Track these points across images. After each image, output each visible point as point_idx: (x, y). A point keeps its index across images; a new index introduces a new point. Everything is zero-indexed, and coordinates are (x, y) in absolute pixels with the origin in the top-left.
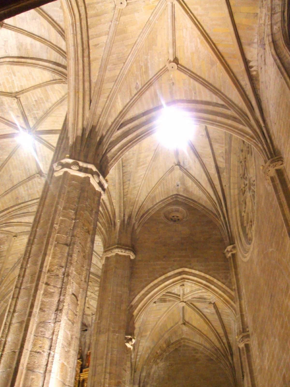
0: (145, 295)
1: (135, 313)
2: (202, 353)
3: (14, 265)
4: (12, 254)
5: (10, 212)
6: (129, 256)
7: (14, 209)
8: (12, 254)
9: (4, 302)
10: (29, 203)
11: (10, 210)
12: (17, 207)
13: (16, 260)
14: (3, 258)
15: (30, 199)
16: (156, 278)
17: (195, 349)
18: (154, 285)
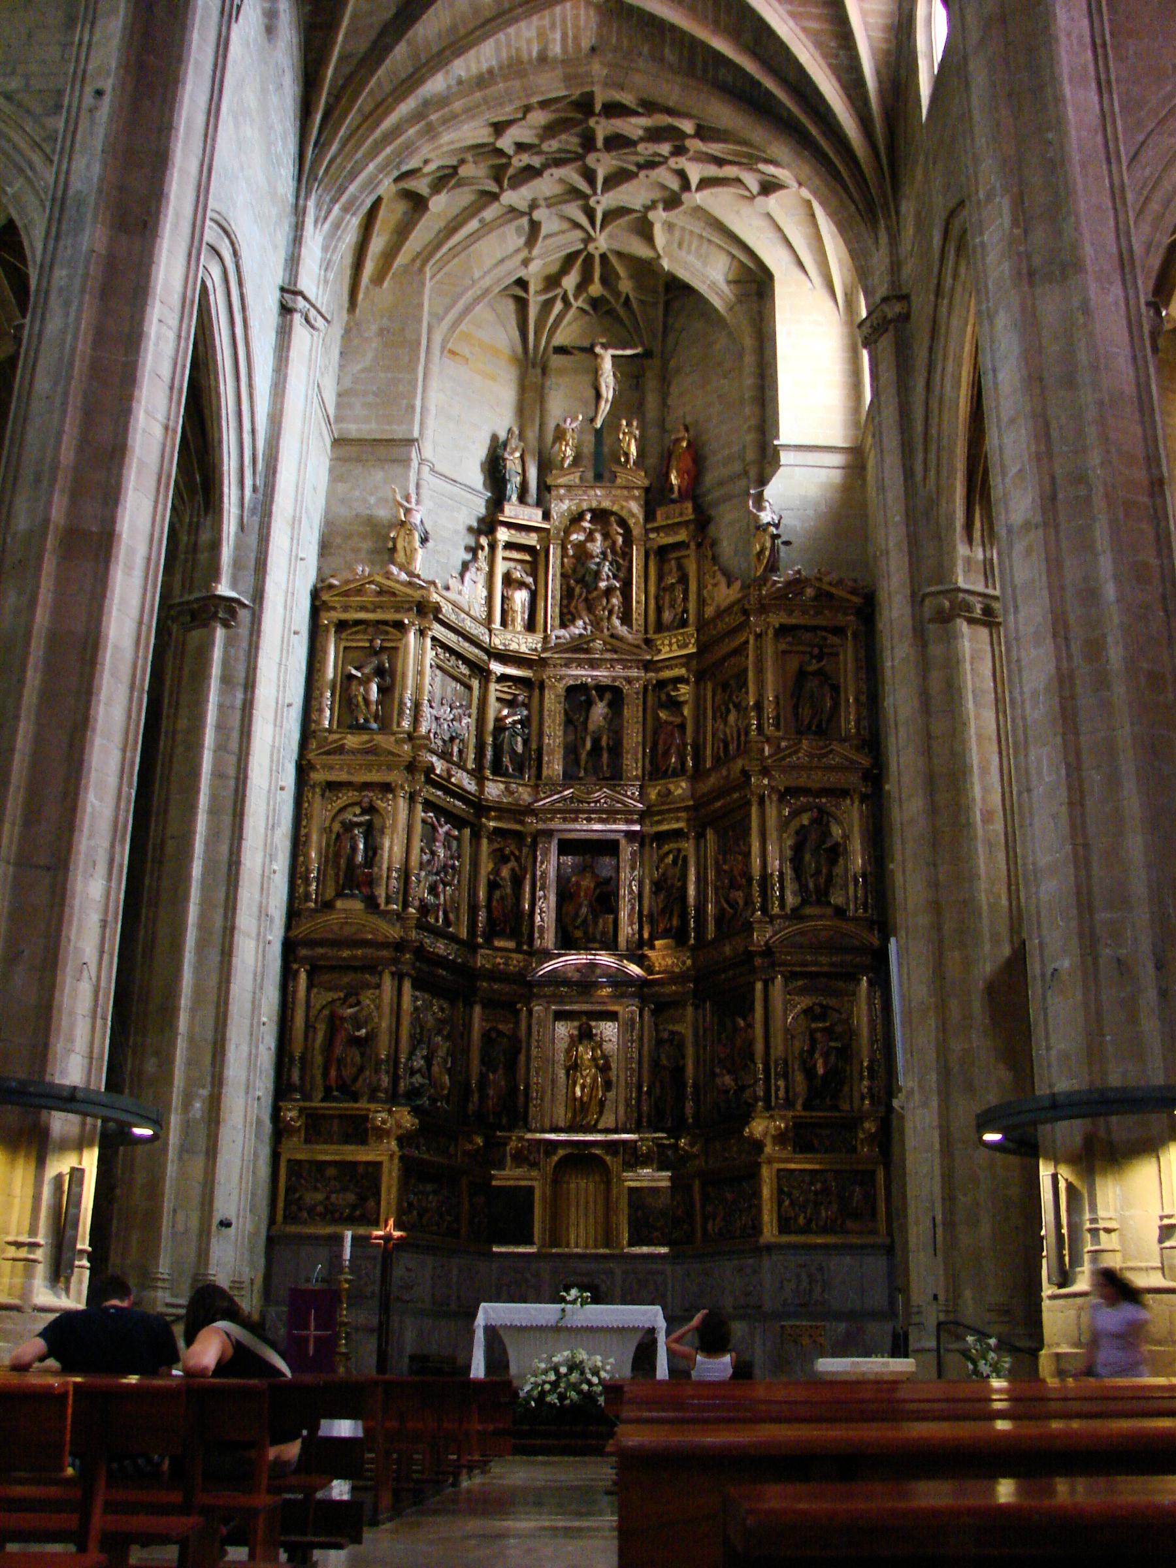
3: (372, 35)
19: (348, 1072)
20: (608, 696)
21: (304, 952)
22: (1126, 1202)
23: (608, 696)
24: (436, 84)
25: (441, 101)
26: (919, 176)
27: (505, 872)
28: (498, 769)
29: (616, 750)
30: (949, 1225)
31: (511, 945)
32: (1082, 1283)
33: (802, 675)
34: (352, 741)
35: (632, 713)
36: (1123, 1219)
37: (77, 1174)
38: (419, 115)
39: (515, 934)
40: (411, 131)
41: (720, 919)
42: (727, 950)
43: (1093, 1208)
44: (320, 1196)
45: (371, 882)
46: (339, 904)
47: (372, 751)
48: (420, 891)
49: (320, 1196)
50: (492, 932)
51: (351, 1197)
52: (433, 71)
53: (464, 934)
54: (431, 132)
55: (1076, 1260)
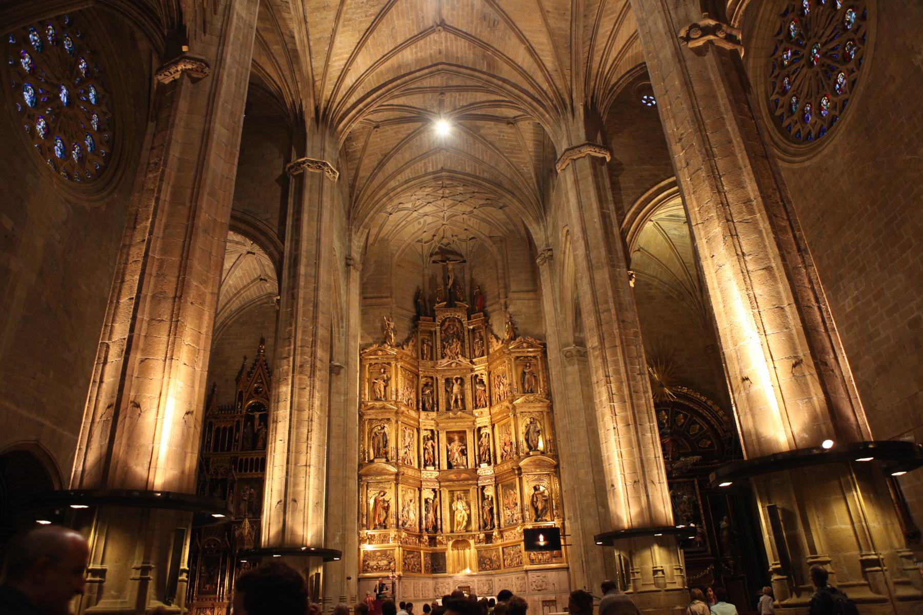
0: (636, 214)
1: (628, 238)
2: (657, 288)
4: (370, 155)
5: (390, 90)
6: (604, 158)
7: (394, 84)
8: (370, 155)
9: (364, 228)
10: (418, 74)
11: (390, 86)
12: (399, 82)
13: (376, 164)
14: (357, 161)
15: (418, 68)
16: (648, 190)
17: (647, 284)
18: (645, 199)
19: (382, 519)
20: (459, 381)
21: (364, 478)
22: (643, 563)
23: (459, 381)
24: (393, 184)
25: (394, 189)
26: (553, 211)
27: (429, 444)
28: (424, 409)
29: (463, 400)
30: (587, 562)
31: (432, 468)
32: (630, 590)
33: (524, 373)
34: (378, 404)
35: (468, 386)
36: (641, 569)
37: (318, 575)
38: (386, 194)
39: (434, 465)
40: (384, 200)
41: (502, 457)
42: (505, 467)
43: (632, 566)
44: (375, 562)
45: (386, 453)
46: (376, 460)
47: (384, 407)
48: (401, 453)
49: (375, 562)
50: (425, 465)
51: (385, 562)
52: (391, 180)
53: (416, 467)
54: (391, 199)
55: (629, 582)
